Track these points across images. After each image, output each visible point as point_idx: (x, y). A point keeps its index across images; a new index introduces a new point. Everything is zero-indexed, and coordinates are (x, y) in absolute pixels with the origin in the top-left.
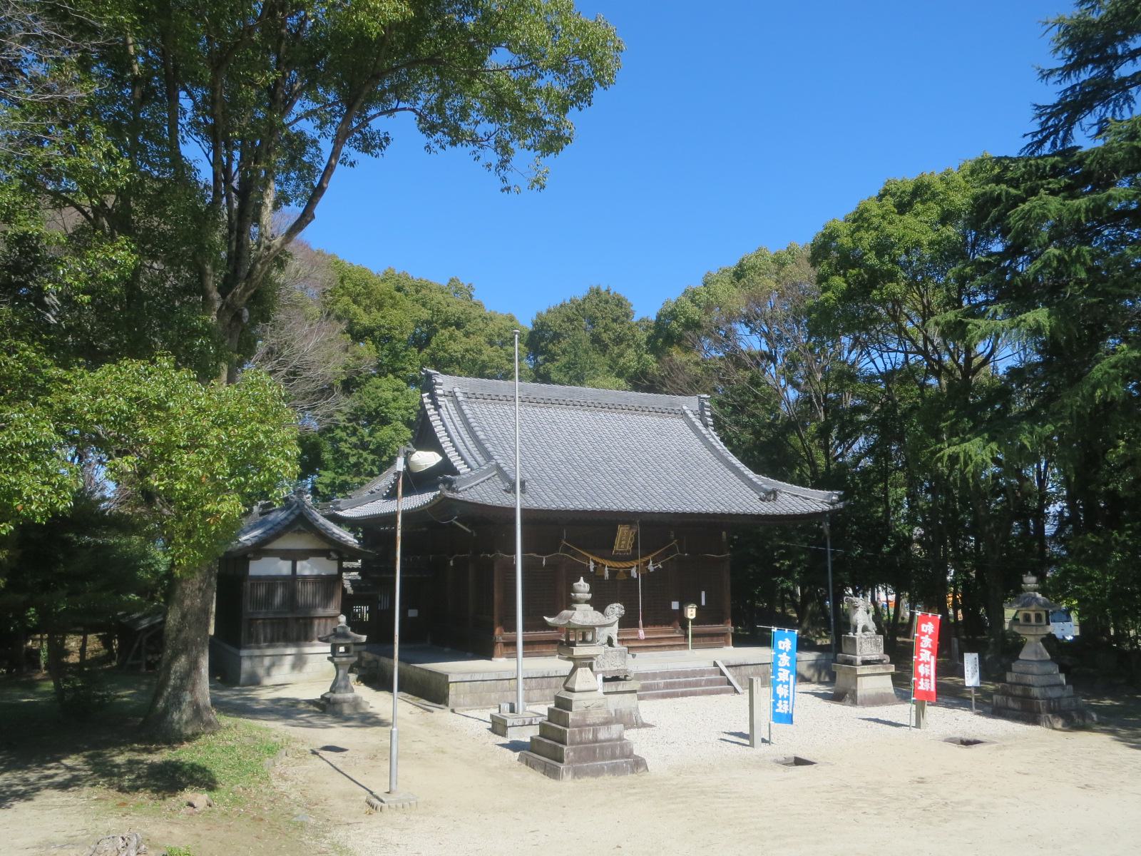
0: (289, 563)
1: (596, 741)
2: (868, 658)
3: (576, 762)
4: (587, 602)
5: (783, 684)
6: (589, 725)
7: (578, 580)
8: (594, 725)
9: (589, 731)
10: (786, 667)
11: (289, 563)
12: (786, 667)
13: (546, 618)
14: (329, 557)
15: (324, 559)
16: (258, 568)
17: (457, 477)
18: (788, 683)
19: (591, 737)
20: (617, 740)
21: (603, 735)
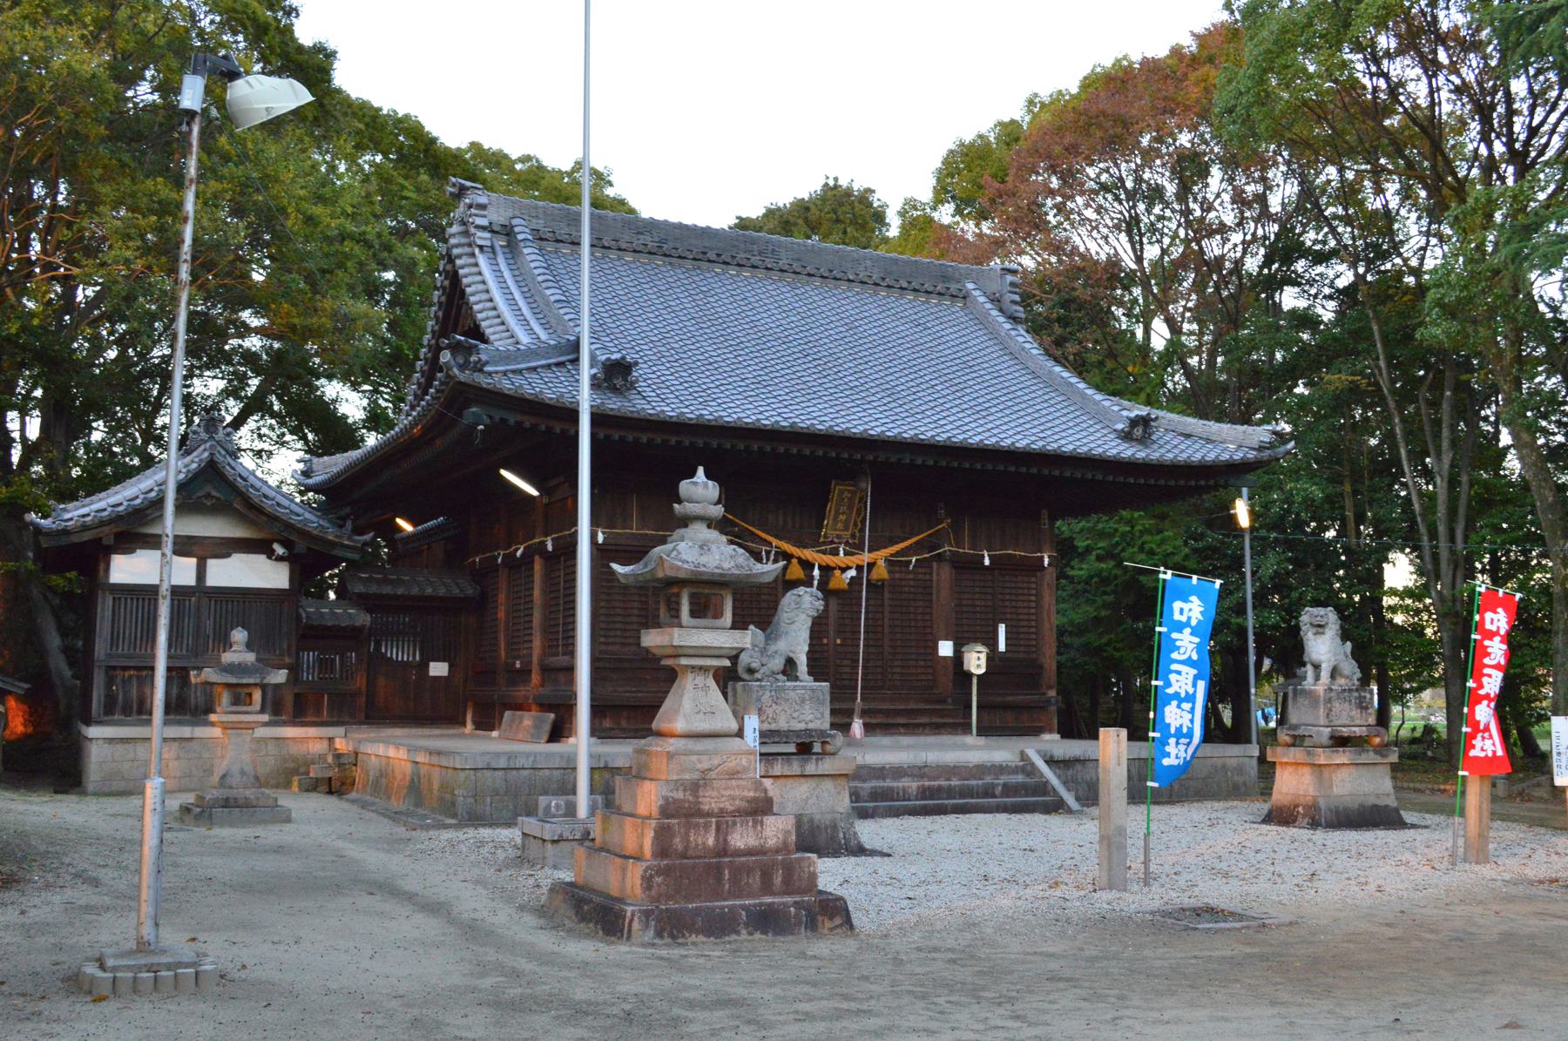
0: (192, 562)
1: (723, 850)
2: (1345, 731)
3: (669, 897)
4: (711, 523)
5: (1181, 701)
6: (709, 814)
7: (692, 474)
8: (722, 812)
9: (707, 826)
10: (1188, 662)
11: (192, 562)
12: (1188, 662)
13: (615, 566)
14: (270, 554)
15: (263, 557)
16: (127, 569)
17: (482, 346)
18: (1190, 698)
19: (711, 841)
20: (777, 851)
21: (741, 839)
